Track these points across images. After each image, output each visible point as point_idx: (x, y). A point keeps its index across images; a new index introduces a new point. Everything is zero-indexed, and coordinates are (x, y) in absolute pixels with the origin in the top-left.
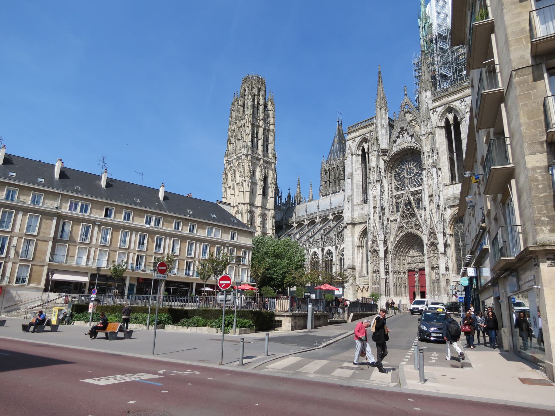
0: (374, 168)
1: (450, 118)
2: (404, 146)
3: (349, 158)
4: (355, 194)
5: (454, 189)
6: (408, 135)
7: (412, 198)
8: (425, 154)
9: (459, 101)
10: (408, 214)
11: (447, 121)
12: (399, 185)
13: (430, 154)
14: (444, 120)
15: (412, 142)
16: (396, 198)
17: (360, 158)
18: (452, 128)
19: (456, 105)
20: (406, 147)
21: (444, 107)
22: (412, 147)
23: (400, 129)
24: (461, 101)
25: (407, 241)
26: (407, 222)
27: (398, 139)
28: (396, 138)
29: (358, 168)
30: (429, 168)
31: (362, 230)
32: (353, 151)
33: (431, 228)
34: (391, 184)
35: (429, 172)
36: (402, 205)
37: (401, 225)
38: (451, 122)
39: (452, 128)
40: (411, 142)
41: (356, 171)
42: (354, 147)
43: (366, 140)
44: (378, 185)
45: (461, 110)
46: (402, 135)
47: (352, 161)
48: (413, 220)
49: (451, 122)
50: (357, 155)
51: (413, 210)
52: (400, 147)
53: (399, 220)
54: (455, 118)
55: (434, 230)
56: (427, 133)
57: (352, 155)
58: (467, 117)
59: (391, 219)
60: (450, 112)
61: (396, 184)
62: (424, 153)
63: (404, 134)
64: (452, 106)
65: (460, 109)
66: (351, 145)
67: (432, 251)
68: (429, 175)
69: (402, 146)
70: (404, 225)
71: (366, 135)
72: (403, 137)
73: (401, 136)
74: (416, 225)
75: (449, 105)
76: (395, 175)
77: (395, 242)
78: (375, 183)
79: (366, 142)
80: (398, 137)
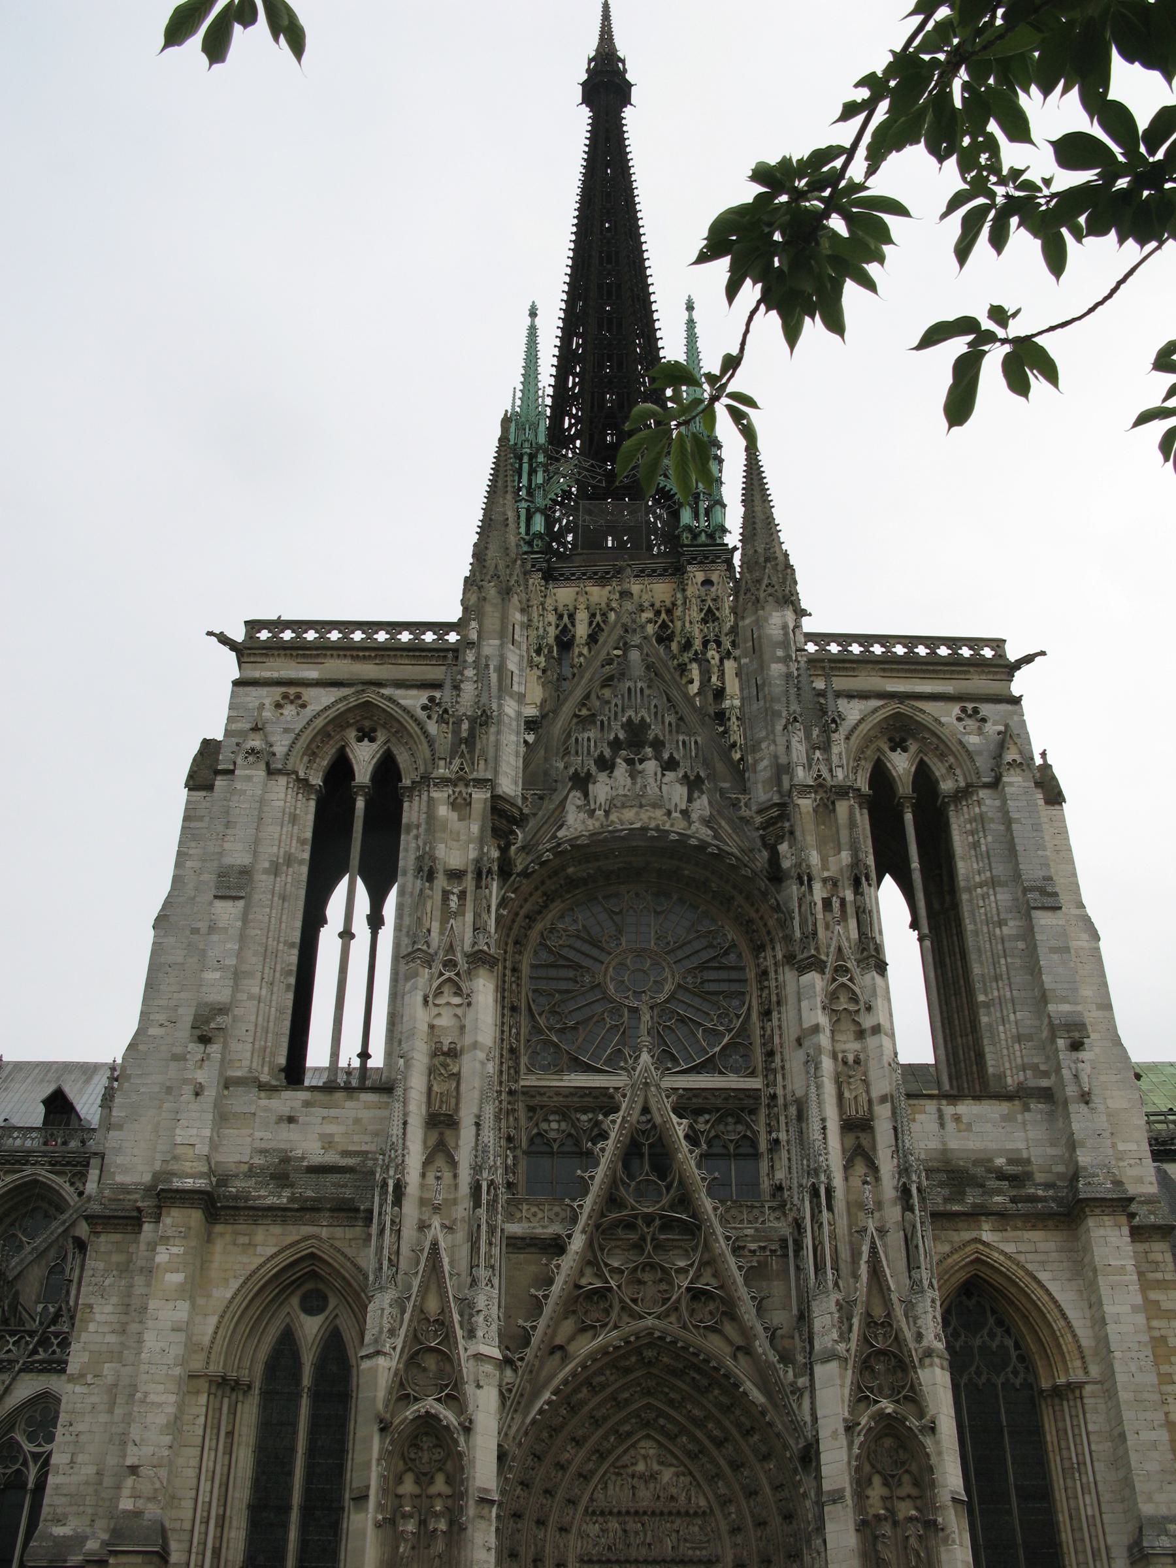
0: (455, 875)
1: (901, 771)
2: (629, 818)
3: (249, 778)
4: (247, 1011)
5: (942, 1125)
6: (670, 776)
7: (679, 1127)
8: (819, 892)
9: (956, 709)
10: (649, 1219)
11: (880, 775)
12: (561, 1031)
13: (849, 895)
14: (869, 766)
15: (694, 816)
16: (531, 1109)
17: (308, 811)
18: (909, 817)
19: (943, 720)
20: (657, 829)
21: (875, 710)
22: (693, 842)
23: (622, 726)
24: (964, 710)
25: (613, 1397)
26: (635, 1269)
27: (602, 777)
28: (593, 770)
29: (289, 860)
30: (841, 970)
31: (272, 1268)
32: (280, 749)
33: (870, 1321)
34: (514, 1009)
35: (843, 985)
36: (608, 1151)
37: (590, 1281)
38: (904, 787)
39: (909, 817)
40: (685, 813)
41: (275, 870)
42: (286, 731)
43: (367, 724)
44: (484, 989)
45: (971, 748)
46: (630, 762)
47: (262, 802)
48: (682, 1264)
49: (904, 787)
50: (298, 780)
51: (685, 1201)
52: (613, 817)
53: (577, 1243)
54: (923, 777)
55: (898, 1340)
56: (821, 785)
57: (271, 772)
58: (1011, 784)
59: (515, 1229)
60: (898, 744)
61: (542, 1021)
62: (810, 879)
63: (641, 761)
64: (920, 717)
65: (961, 742)
66: (267, 714)
67: (877, 1480)
68: (843, 1003)
69: (629, 814)
70: (613, 1284)
71: (386, 691)
72: (633, 775)
73: (621, 768)
74: (696, 1295)
75: (903, 709)
76: (533, 966)
77: (536, 1394)
78: (463, 965)
79: (366, 735)
80: (605, 765)
